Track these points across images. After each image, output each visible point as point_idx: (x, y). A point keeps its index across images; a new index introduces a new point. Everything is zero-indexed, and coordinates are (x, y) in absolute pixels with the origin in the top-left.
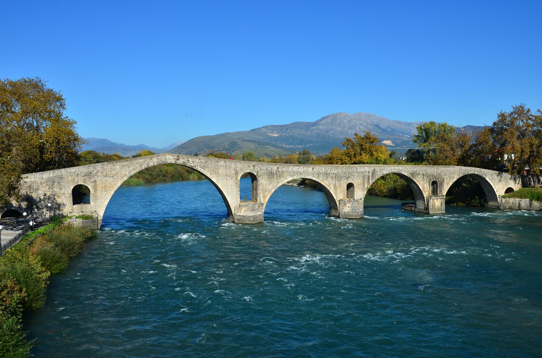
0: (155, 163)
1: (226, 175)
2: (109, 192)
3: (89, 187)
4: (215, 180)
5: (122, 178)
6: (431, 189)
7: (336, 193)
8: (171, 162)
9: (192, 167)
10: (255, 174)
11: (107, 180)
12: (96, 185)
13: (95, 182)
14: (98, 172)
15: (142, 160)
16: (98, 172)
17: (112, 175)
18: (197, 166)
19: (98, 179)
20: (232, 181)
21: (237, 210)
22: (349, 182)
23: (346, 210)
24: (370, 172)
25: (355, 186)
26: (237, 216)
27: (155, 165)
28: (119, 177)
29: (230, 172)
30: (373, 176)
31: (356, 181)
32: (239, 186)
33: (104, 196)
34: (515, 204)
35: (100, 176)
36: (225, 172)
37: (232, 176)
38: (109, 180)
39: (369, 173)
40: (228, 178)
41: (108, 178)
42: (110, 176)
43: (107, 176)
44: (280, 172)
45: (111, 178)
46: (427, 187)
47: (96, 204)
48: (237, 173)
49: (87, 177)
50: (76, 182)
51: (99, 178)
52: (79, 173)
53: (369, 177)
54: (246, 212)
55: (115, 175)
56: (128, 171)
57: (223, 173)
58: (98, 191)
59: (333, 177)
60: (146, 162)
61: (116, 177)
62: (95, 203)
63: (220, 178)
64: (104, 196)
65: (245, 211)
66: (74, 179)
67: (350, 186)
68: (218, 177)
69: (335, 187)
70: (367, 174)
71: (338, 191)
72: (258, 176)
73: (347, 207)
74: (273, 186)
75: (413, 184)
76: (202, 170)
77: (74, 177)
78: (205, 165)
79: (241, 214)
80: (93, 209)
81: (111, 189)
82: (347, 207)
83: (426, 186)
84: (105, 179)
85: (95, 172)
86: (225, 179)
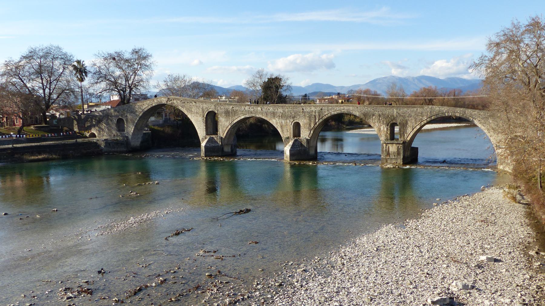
6: (389, 132)
7: (282, 131)
10: (216, 112)
22: (295, 121)
24: (317, 111)
25: (301, 125)
30: (319, 115)
31: (303, 122)
36: (196, 111)
39: (315, 113)
40: (198, 115)
59: (279, 116)
63: (193, 115)
67: (297, 126)
69: (281, 127)
70: (314, 113)
71: (285, 131)
76: (182, 109)
83: (382, 129)
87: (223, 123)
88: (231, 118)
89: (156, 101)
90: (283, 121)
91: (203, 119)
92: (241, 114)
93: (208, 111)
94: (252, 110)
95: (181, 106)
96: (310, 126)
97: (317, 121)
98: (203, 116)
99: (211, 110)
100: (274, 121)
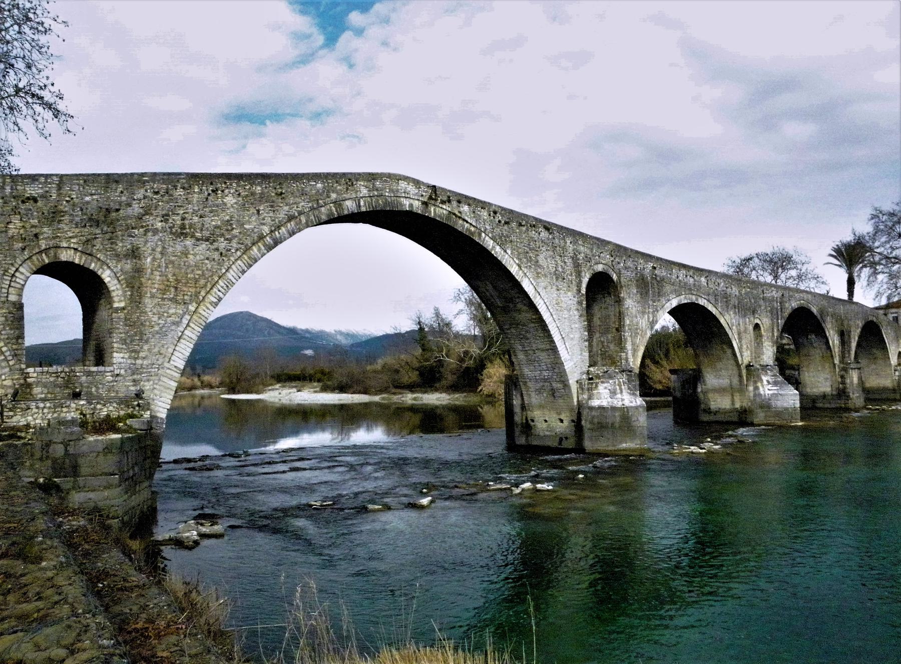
0: (362, 203)
1: (558, 276)
2: (192, 308)
3: (106, 276)
4: (531, 287)
5: (247, 249)
8: (411, 205)
9: (472, 233)
10: (615, 277)
11: (185, 254)
12: (138, 271)
13: (134, 253)
14: (147, 212)
15: (319, 185)
16: (147, 212)
17: (206, 234)
18: (483, 235)
19: (149, 245)
20: (569, 294)
21: (588, 389)
23: (767, 392)
26: (592, 408)
27: (363, 209)
28: (234, 244)
29: (562, 264)
30: (781, 309)
32: (585, 313)
33: (174, 323)
35: (156, 232)
38: (195, 255)
40: (560, 284)
41: (189, 242)
42: (198, 235)
43: (185, 235)
44: (658, 278)
45: (204, 246)
47: (139, 362)
48: (579, 274)
49: (98, 231)
50: (46, 251)
51: (153, 239)
52: (64, 206)
54: (619, 396)
55: (218, 231)
56: (268, 220)
57: (548, 267)
58: (147, 300)
60: (334, 196)
61: (222, 244)
62: (135, 353)
63: (543, 282)
64: (174, 323)
65: (613, 393)
66: (35, 231)
68: (538, 277)
69: (739, 334)
73: (765, 383)
74: (648, 317)
76: (498, 248)
77: (35, 222)
78: (505, 233)
80: (127, 388)
81: (203, 293)
82: (765, 383)
84: (179, 248)
85: (136, 209)
86: (555, 287)
88: (651, 303)
89: (364, 191)
91: (580, 303)
92: (671, 293)
94: (692, 280)
95: (493, 239)
96: (773, 334)
98: (579, 291)
99: (600, 268)
100: (727, 317)
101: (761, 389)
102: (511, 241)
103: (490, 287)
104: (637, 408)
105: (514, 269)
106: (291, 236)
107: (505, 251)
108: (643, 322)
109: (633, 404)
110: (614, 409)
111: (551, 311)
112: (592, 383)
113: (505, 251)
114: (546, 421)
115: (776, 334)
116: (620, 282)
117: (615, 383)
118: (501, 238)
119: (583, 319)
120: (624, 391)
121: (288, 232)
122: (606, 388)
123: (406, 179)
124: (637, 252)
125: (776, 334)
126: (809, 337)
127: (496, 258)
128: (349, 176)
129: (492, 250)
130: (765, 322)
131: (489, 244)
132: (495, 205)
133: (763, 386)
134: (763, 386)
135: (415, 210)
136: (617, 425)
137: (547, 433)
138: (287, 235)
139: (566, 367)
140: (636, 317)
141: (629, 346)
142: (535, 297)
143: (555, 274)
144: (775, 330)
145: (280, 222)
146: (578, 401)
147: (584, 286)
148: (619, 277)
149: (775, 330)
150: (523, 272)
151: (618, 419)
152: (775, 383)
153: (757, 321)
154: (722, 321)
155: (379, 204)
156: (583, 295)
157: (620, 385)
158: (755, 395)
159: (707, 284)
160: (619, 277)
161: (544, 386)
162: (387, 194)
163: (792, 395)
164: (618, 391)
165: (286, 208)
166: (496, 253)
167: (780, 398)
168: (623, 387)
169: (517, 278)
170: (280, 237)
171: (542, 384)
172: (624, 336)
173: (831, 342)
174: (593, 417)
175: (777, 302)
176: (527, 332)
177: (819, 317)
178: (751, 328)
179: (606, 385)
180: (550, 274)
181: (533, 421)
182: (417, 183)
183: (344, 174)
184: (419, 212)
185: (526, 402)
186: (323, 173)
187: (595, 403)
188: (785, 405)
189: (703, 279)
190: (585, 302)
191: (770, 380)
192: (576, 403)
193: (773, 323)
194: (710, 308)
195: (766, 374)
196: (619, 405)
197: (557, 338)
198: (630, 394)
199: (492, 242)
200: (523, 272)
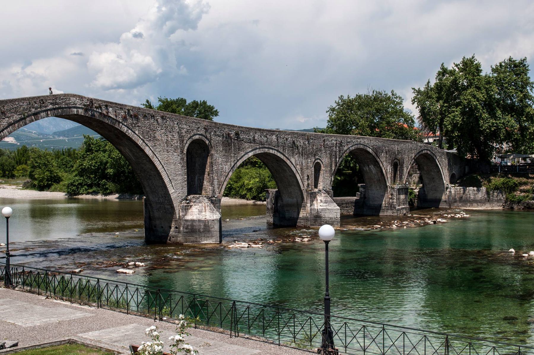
6: (393, 175)
10: (207, 142)
20: (175, 154)
23: (319, 207)
26: (187, 221)
31: (325, 160)
34: (468, 196)
37: (176, 144)
46: (389, 171)
53: (336, 154)
54: (204, 213)
65: (200, 212)
72: (212, 147)
73: (319, 201)
74: (231, 165)
75: (372, 167)
76: (130, 131)
79: (195, 218)
82: (319, 201)
87: (221, 166)
88: (232, 155)
90: (304, 161)
91: (182, 159)
93: (191, 140)
97: (337, 159)
99: (197, 137)
101: (316, 205)
102: (138, 126)
103: (127, 150)
104: (213, 220)
105: (140, 142)
106: (9, 134)
107: (134, 133)
108: (227, 168)
109: (212, 218)
110: (199, 221)
111: (163, 165)
112: (188, 206)
113: (134, 133)
114: (162, 227)
115: (333, 168)
116: (211, 144)
117: (202, 205)
118: (132, 125)
119: (183, 168)
120: (207, 210)
121: (8, 132)
122: (196, 209)
123: (74, 96)
124: (224, 125)
125: (333, 168)
126: (370, 166)
127: (129, 137)
128: (42, 98)
129: (126, 132)
130: (325, 160)
131: (125, 129)
132: (129, 106)
133: (317, 203)
134: (317, 203)
135: (80, 113)
136: (202, 230)
137: (163, 234)
138: (7, 134)
139: (172, 197)
140: (221, 164)
141: (216, 182)
142: (153, 158)
143: (166, 143)
144: (333, 166)
145: (3, 126)
146: (179, 216)
147: (186, 148)
148: (210, 142)
149: (333, 166)
150: (146, 143)
151: (202, 227)
152: (326, 202)
153: (319, 161)
154: (288, 162)
155: (59, 112)
156: (185, 154)
157: (205, 207)
158: (311, 210)
159: (277, 140)
160: (210, 142)
161: (160, 207)
162: (63, 106)
163: (335, 209)
164: (204, 210)
165: (7, 119)
166: (129, 134)
167: (327, 211)
168: (207, 208)
169: (142, 147)
170: (4, 135)
171: (159, 205)
172: (212, 176)
173: (384, 171)
174: (188, 226)
175: (336, 148)
176: (150, 176)
177: (374, 154)
178: (311, 165)
179: (196, 207)
180: (163, 143)
181: (155, 227)
182: (81, 98)
183: (39, 97)
184: (83, 114)
185: (151, 216)
186: (27, 98)
187: (189, 217)
188: (331, 216)
189: (274, 137)
190: (185, 158)
191: (323, 200)
192: (178, 218)
193: (331, 162)
194: (279, 155)
195: (321, 196)
196: (202, 218)
197: (166, 180)
198: (210, 212)
199: (126, 128)
200: (146, 143)
